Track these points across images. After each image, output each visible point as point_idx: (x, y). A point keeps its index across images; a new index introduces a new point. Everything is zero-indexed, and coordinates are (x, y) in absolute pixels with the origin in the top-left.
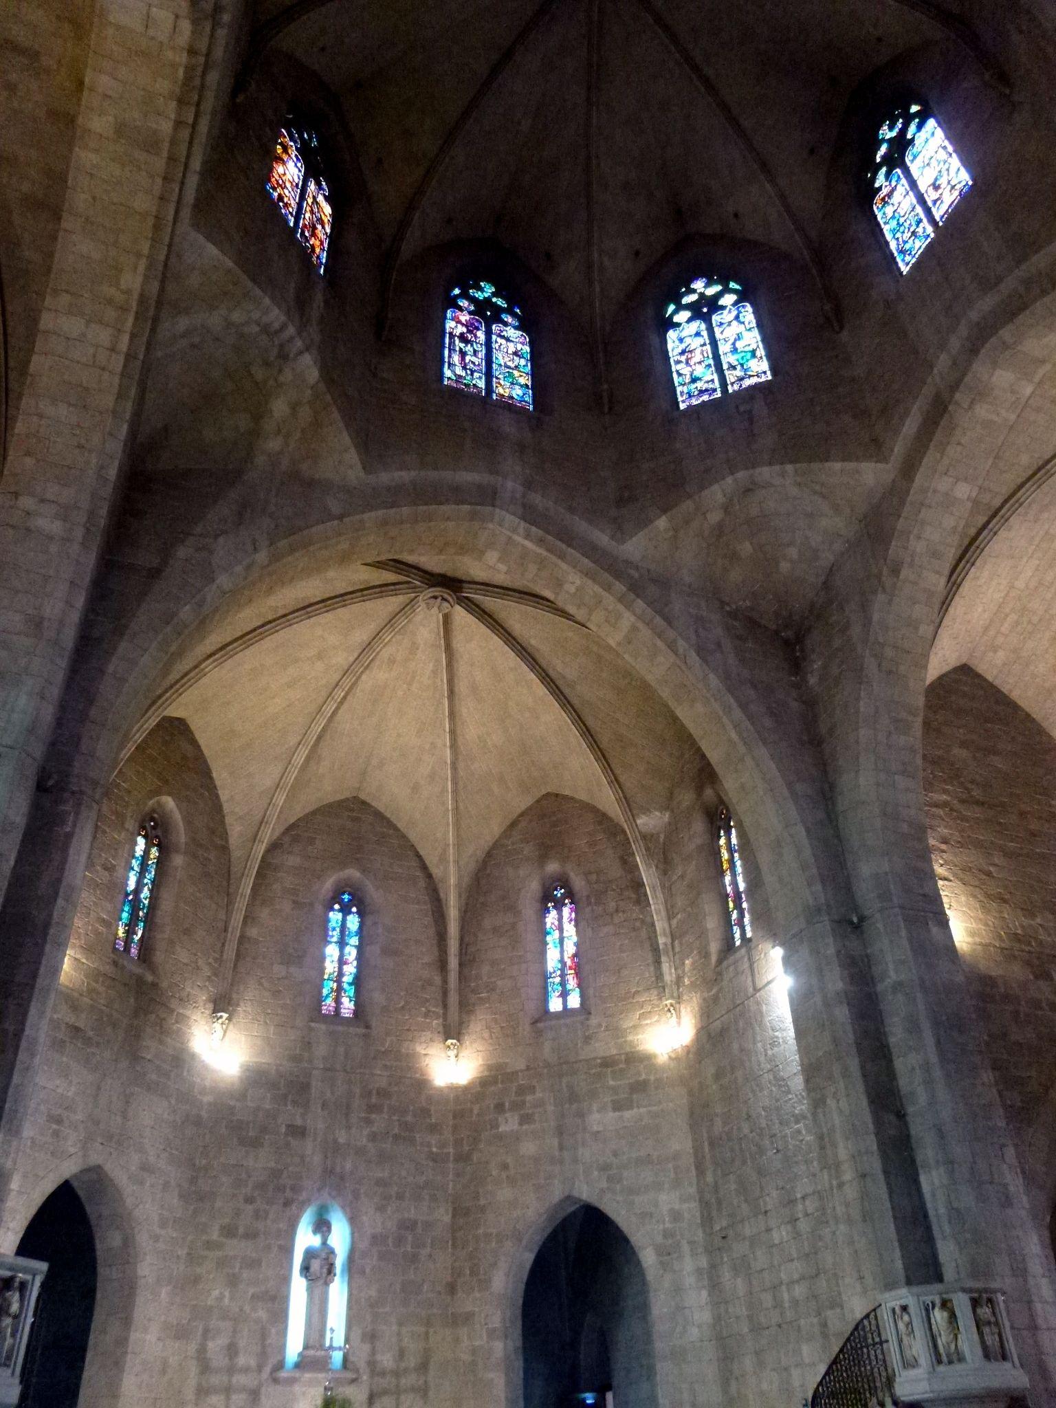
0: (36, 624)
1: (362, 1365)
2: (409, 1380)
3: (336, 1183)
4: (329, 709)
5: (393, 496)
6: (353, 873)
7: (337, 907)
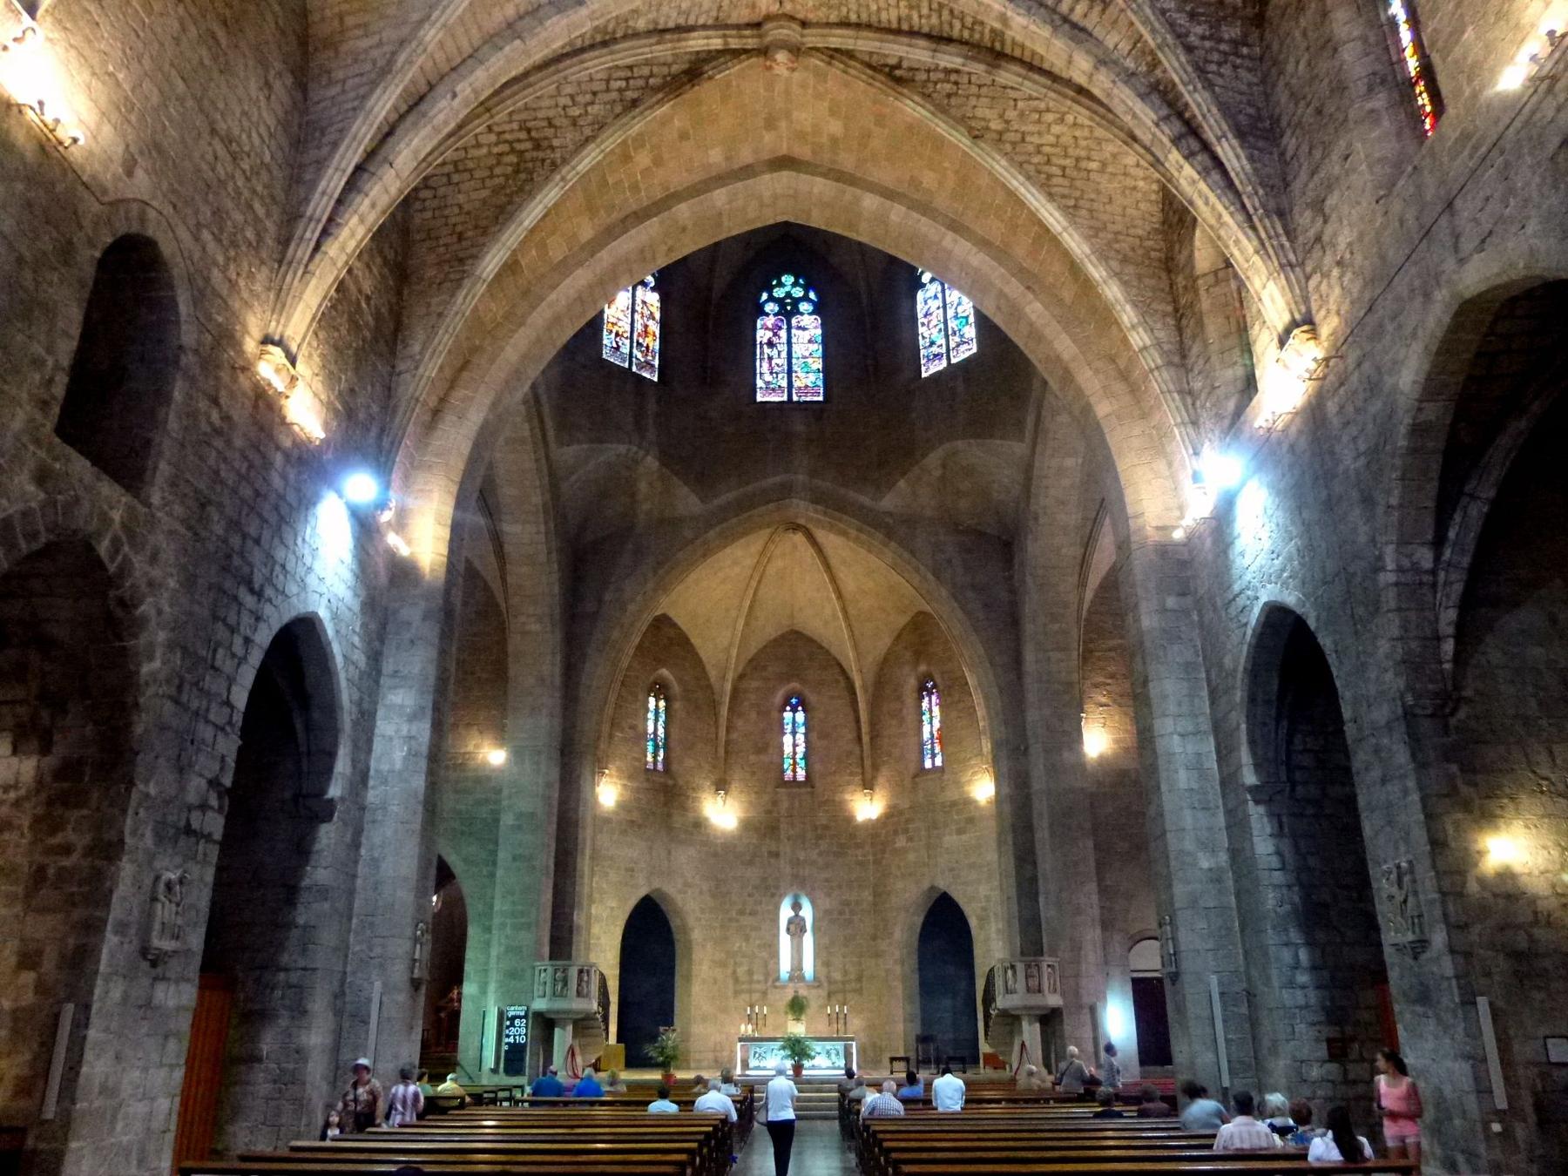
1: (823, 979)
3: (801, 884)
4: (754, 584)
5: (723, 514)
6: (795, 685)
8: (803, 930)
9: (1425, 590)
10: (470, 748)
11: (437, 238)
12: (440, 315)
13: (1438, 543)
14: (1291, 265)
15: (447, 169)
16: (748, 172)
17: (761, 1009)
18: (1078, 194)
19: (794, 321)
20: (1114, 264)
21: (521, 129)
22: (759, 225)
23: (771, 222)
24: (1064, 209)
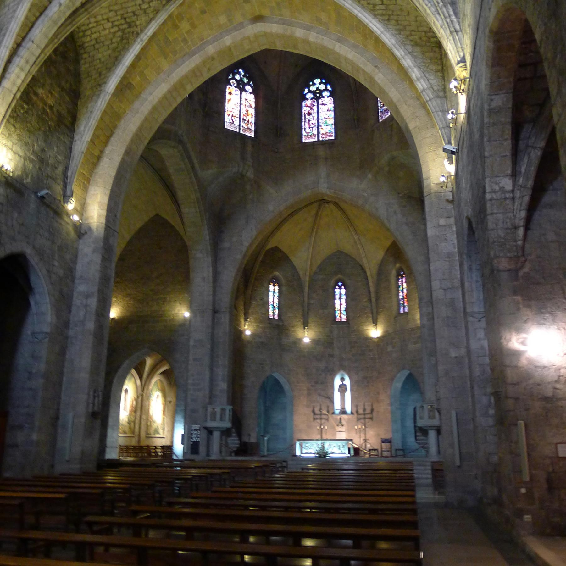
0: (204, 278)
2: (367, 416)
6: (340, 276)
7: (337, 287)
8: (346, 390)
9: (508, 202)
10: (176, 311)
11: (91, 76)
12: (91, 112)
13: (514, 175)
14: (456, 31)
15: (93, 42)
16: (241, 26)
17: (324, 427)
18: (390, 13)
19: (320, 101)
20: (409, 48)
21: (121, 19)
22: (253, 52)
23: (259, 50)
24: (382, 21)
